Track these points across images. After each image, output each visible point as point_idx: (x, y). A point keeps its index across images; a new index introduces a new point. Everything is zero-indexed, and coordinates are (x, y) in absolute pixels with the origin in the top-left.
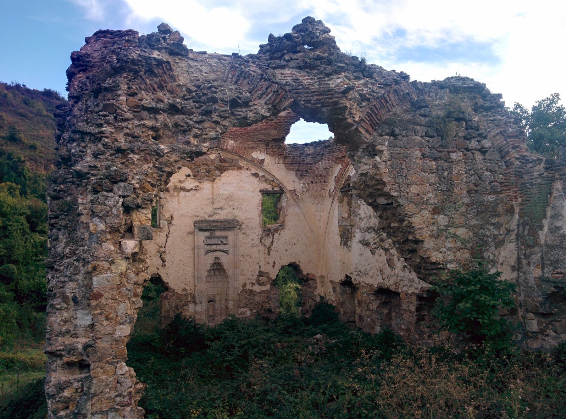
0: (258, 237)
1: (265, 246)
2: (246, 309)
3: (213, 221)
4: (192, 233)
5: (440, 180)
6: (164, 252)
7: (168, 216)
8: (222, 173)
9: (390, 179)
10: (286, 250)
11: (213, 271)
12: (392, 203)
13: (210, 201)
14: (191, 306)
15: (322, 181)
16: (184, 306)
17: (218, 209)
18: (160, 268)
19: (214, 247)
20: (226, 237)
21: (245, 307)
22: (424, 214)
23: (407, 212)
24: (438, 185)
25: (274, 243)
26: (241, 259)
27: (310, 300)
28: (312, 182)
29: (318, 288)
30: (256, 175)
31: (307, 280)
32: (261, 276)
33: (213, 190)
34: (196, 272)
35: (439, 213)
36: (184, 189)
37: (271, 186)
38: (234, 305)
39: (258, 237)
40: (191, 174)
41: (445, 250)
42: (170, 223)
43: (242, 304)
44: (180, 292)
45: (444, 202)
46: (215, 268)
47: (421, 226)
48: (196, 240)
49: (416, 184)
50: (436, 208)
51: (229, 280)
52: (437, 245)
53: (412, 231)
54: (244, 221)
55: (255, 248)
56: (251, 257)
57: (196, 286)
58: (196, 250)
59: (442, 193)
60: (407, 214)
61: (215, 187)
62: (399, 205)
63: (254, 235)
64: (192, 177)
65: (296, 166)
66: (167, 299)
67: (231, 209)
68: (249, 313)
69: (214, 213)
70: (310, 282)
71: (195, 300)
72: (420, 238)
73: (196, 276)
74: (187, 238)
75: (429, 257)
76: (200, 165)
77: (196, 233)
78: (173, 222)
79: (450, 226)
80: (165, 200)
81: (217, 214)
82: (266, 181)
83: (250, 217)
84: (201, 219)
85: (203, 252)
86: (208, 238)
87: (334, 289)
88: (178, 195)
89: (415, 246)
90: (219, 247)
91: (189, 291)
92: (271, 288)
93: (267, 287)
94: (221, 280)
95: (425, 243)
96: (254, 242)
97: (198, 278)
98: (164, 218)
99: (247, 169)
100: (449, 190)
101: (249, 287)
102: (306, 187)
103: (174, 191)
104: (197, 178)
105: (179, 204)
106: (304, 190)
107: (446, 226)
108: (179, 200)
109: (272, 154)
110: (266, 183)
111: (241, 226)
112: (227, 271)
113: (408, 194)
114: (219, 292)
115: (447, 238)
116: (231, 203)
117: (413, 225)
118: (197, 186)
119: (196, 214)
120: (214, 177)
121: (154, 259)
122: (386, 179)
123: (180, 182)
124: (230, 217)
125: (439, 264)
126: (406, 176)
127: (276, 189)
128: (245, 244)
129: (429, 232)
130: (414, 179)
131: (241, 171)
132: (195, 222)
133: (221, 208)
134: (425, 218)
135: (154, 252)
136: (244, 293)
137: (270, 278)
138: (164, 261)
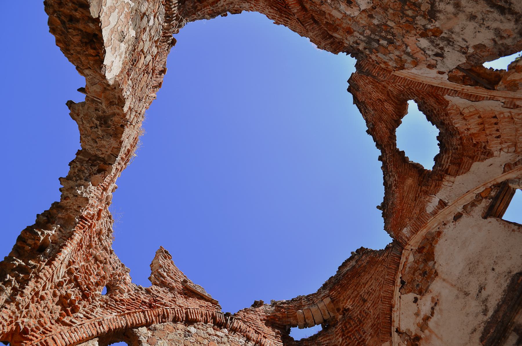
13: (461, 295)
15: (494, 121)
17: (480, 292)
28: (498, 137)
30: (457, 217)
33: (448, 282)
36: (427, 319)
37: (484, 200)
61: (446, 277)
64: (418, 296)
65: (465, 159)
67: (491, 275)
69: (483, 302)
76: (412, 279)
81: (486, 299)
82: (473, 204)
84: (482, 328)
88: (430, 331)
99: (445, 224)
102: (509, 147)
103: (423, 332)
105: (442, 340)
106: (512, 149)
108: (436, 335)
109: (438, 187)
110: (476, 206)
118: (433, 299)
119: (470, 330)
120: (434, 271)
123: (417, 314)
127: (493, 194)
131: (443, 234)
133: (481, 288)
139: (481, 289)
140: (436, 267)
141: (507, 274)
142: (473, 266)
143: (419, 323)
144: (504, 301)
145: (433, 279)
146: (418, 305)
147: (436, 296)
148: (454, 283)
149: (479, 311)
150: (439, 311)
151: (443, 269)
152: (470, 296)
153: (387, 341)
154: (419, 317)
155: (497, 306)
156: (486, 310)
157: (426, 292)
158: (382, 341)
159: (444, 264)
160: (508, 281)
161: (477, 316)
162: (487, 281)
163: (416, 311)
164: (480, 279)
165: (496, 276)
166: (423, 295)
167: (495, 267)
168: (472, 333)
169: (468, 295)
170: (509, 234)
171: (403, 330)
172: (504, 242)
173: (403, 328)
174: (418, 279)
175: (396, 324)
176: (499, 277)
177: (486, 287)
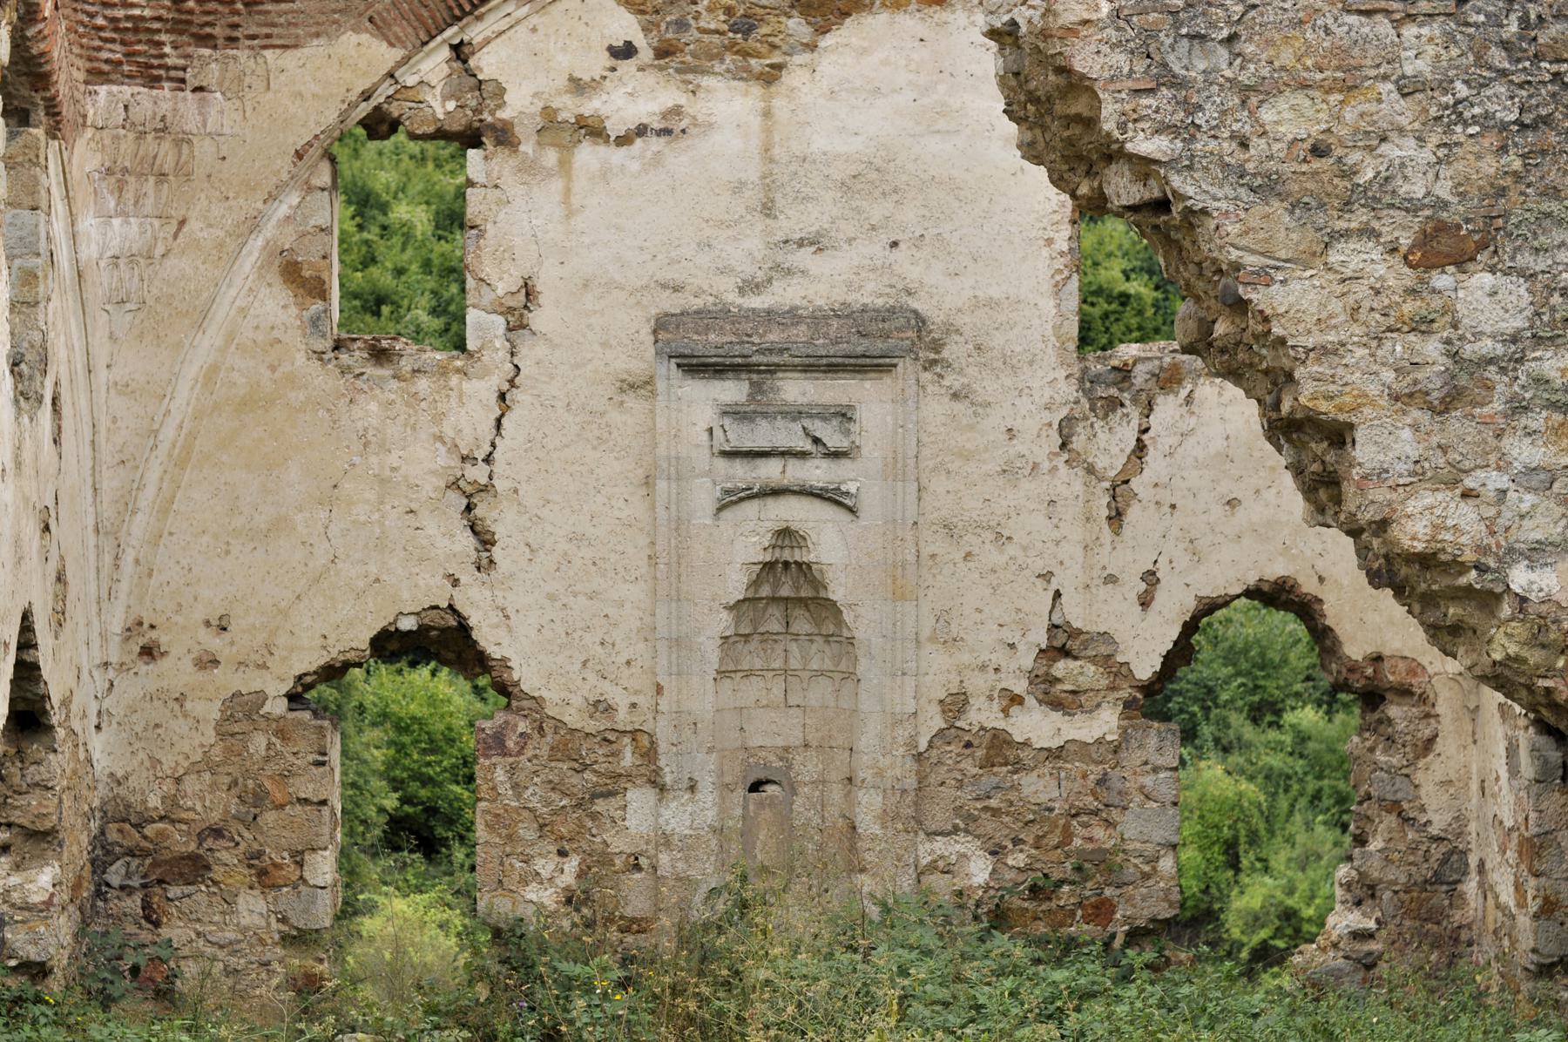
0: (1047, 416)
1: (1091, 470)
2: (961, 845)
3: (770, 315)
4: (640, 386)
5: (1480, 61)
6: (484, 489)
7: (505, 284)
8: (823, 31)
9: (1120, 59)
10: (1232, 503)
11: (776, 611)
12: (1162, 205)
13: (753, 196)
14: (639, 799)
16: (594, 796)
18: (463, 579)
19: (770, 471)
20: (844, 415)
21: (956, 829)
22: (1355, 263)
23: (1234, 254)
24: (1462, 90)
25: (1152, 456)
26: (935, 544)
27: (1391, 820)
29: (1439, 746)
31: (1372, 698)
32: (1065, 652)
33: (768, 131)
34: (661, 612)
35: (1462, 261)
36: (592, 129)
38: (887, 817)
39: (1047, 416)
40: (640, 41)
41: (1497, 480)
42: (517, 324)
43: (939, 816)
44: (573, 718)
45: (1502, 192)
46: (785, 591)
47: (1332, 337)
48: (661, 423)
49: (1304, 86)
50: (1442, 228)
51: (861, 669)
52: (1443, 449)
53: (1286, 363)
54: (959, 320)
55: (1025, 485)
56: (1002, 539)
57: (659, 690)
58: (662, 485)
59: (1491, 140)
60: (1237, 267)
62: (1189, 212)
63: (1024, 404)
64: (646, 54)
66: (505, 753)
67: (875, 249)
68: (979, 871)
69: (777, 267)
70: (1394, 711)
71: (658, 771)
72: (1323, 406)
73: (662, 631)
74: (614, 416)
75: (1382, 525)
77: (661, 385)
78: (538, 319)
79: (1538, 340)
80: (493, 194)
81: (789, 272)
83: (996, 292)
84: (698, 303)
85: (704, 496)
86: (734, 413)
87: (1512, 751)
88: (565, 165)
89: (1330, 458)
90: (800, 473)
91: (623, 719)
92: (1124, 732)
93: (1105, 722)
94: (828, 665)
95: (1359, 435)
96: (1019, 446)
97: (677, 643)
98: (488, 297)
100: (1546, 120)
101: (983, 715)
103: (539, 143)
104: (674, 62)
105: (570, 214)
107: (1515, 339)
108: (568, 191)
111: (937, 346)
112: (847, 617)
113: (1244, 145)
114: (814, 739)
115: (1518, 408)
116: (877, 212)
117: (1277, 330)
118: (676, 111)
120: (776, 58)
121: (431, 525)
122: (1087, 59)
123: (578, 86)
124: (870, 295)
125: (1463, 568)
126: (1232, 39)
128: (966, 456)
129: (1388, 375)
130: (1286, 57)
132: (662, 324)
133: (815, 243)
134: (1361, 290)
135: (431, 486)
136: (955, 748)
137: (1118, 671)
138: (485, 540)
139: (812, 244)
140: (798, 59)
141: (900, 286)
142: (872, 183)
143: (556, 111)
144: (818, 319)
145: (743, 74)
146: (613, 69)
147: (694, 118)
148: (777, 151)
149: (740, 269)
150: (649, 154)
151: (805, 89)
152: (768, 221)
153: (391, 45)
154: (578, 100)
155: (787, 308)
156: (757, 286)
157: (678, 71)
158: (371, 20)
159: (825, 83)
160: (880, 302)
161: (722, 271)
162: (846, 246)
163: (587, 78)
164: (842, 224)
165: (879, 263)
166: (661, 69)
167: (902, 246)
168: (664, 286)
169: (768, 216)
170: (1034, 234)
171: (481, 70)
172: (998, 234)
173: (487, 63)
174: (710, 10)
175: (475, 32)
176: (879, 273)
177: (826, 252)
